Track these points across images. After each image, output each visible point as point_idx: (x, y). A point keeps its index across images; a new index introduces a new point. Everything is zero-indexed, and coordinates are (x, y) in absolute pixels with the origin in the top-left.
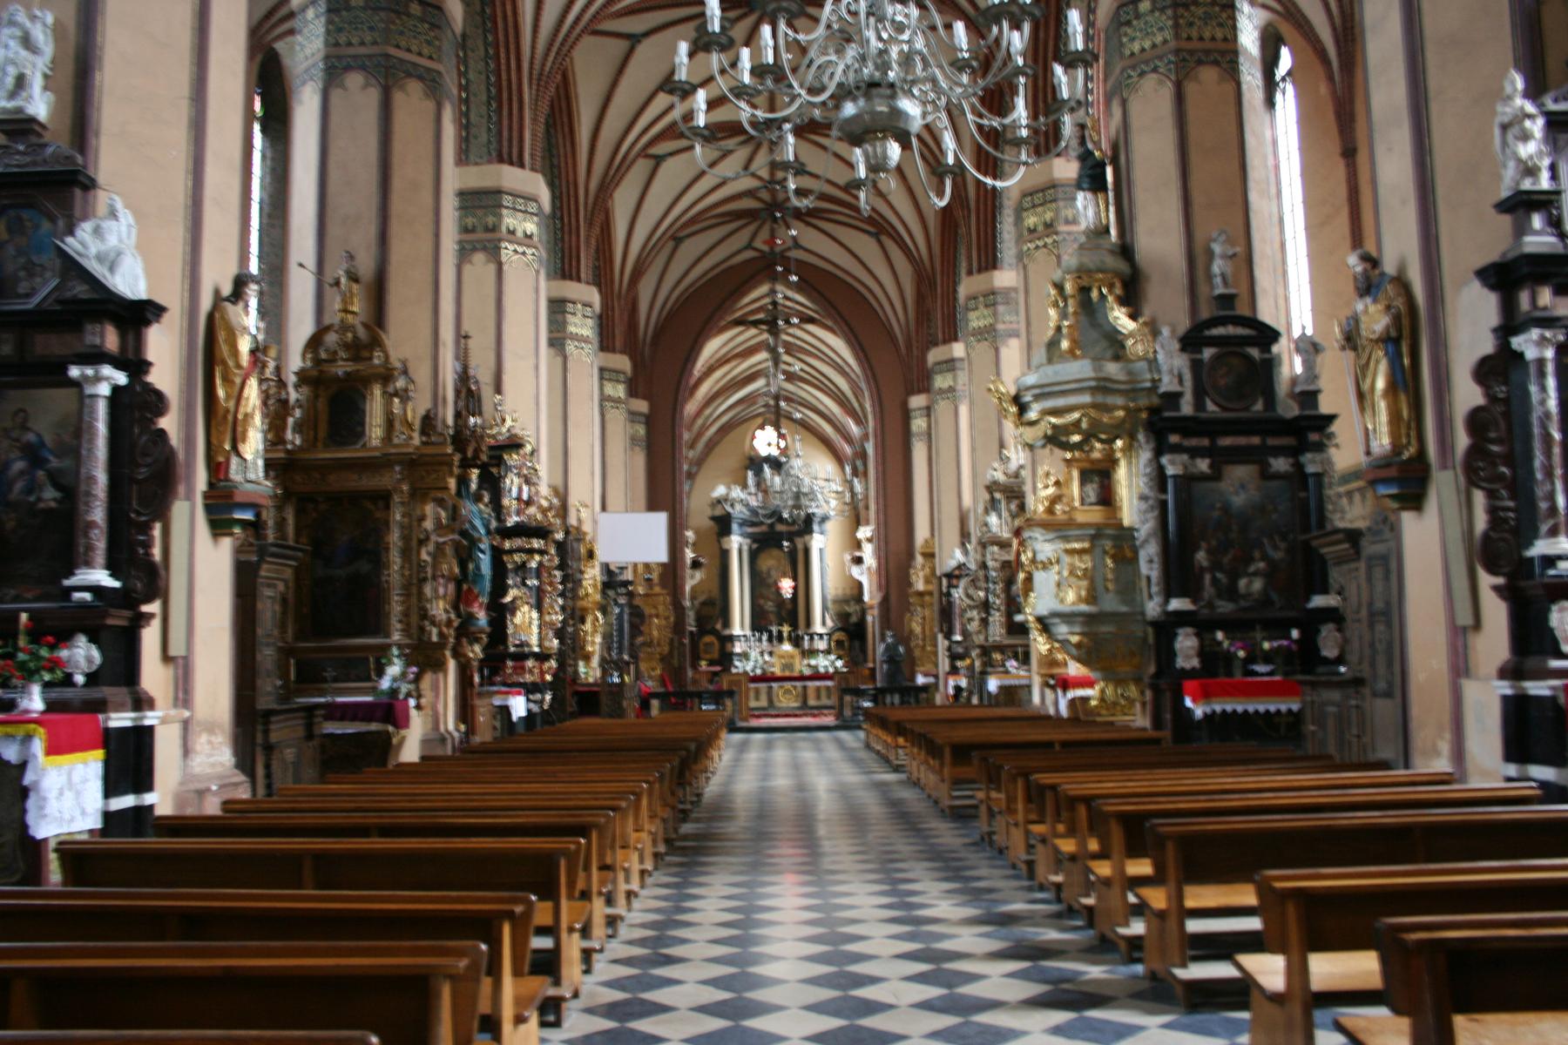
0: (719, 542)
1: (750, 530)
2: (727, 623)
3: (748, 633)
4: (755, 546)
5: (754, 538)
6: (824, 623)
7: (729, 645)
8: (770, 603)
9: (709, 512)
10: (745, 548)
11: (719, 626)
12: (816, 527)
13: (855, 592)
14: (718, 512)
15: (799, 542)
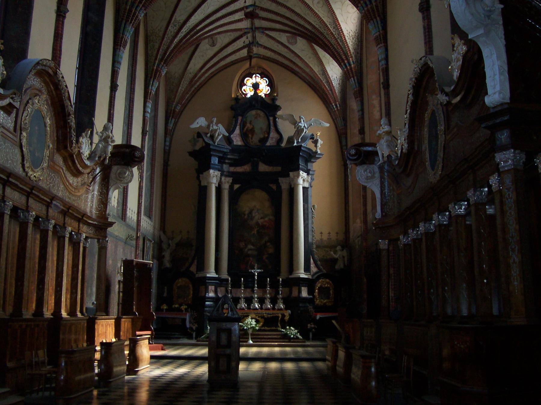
0: (198, 178)
1: (232, 169)
2: (202, 266)
3: (225, 275)
4: (236, 186)
5: (236, 178)
6: (307, 269)
7: (202, 288)
8: (250, 247)
9: (190, 149)
10: (226, 187)
11: (193, 268)
12: (301, 163)
13: (341, 237)
14: (199, 145)
15: (284, 183)
